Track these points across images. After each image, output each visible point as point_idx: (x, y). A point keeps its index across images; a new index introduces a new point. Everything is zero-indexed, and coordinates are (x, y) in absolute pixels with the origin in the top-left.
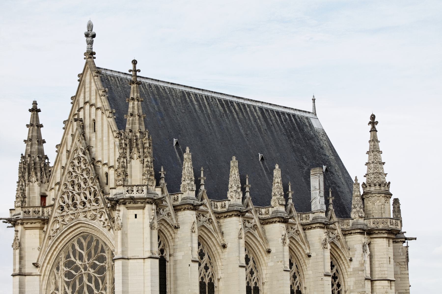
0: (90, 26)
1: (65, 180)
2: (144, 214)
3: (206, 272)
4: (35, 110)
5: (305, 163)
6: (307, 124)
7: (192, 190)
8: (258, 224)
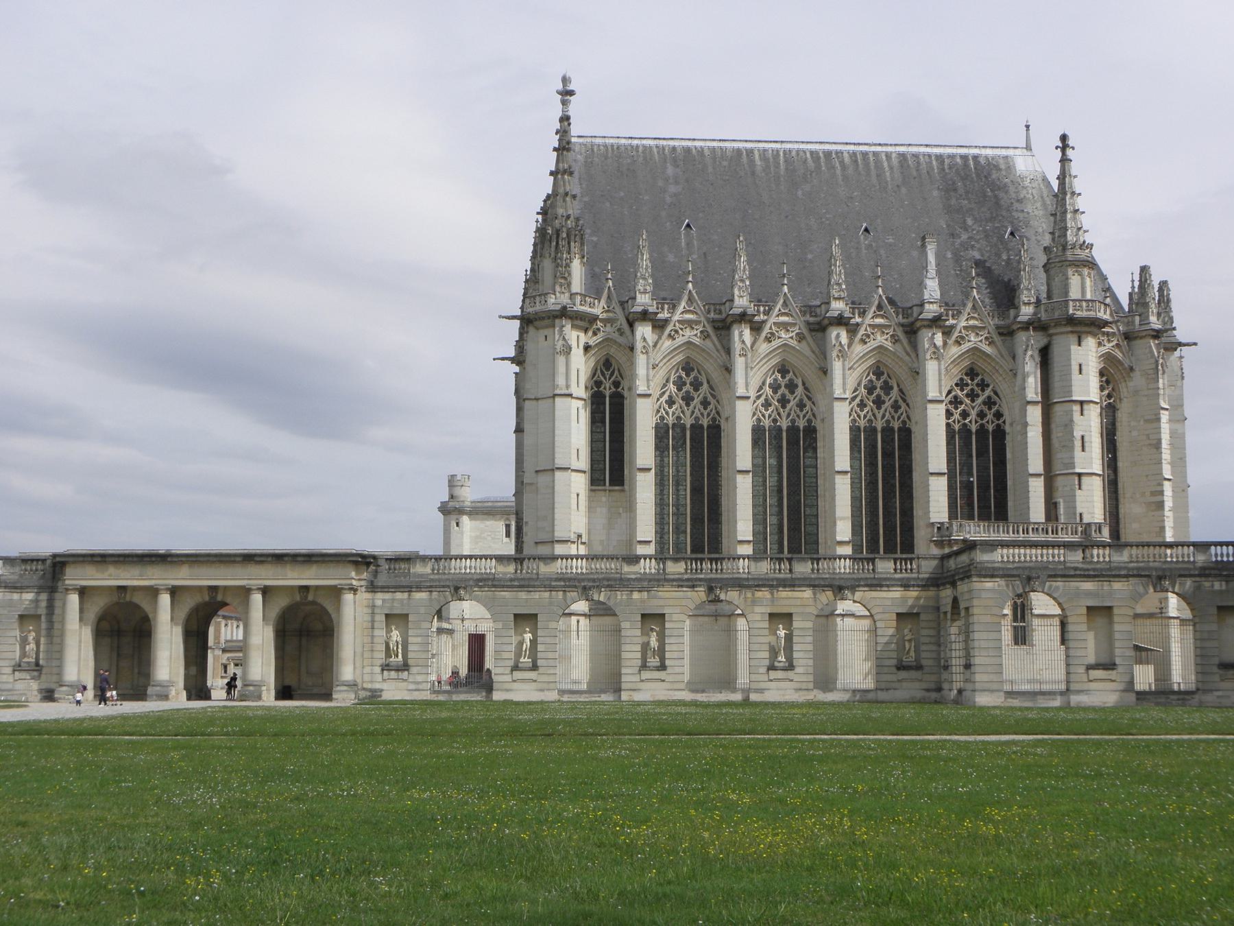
0: (565, 80)
3: (705, 409)
5: (966, 228)
6: (1003, 167)
7: (645, 292)
8: (805, 331)
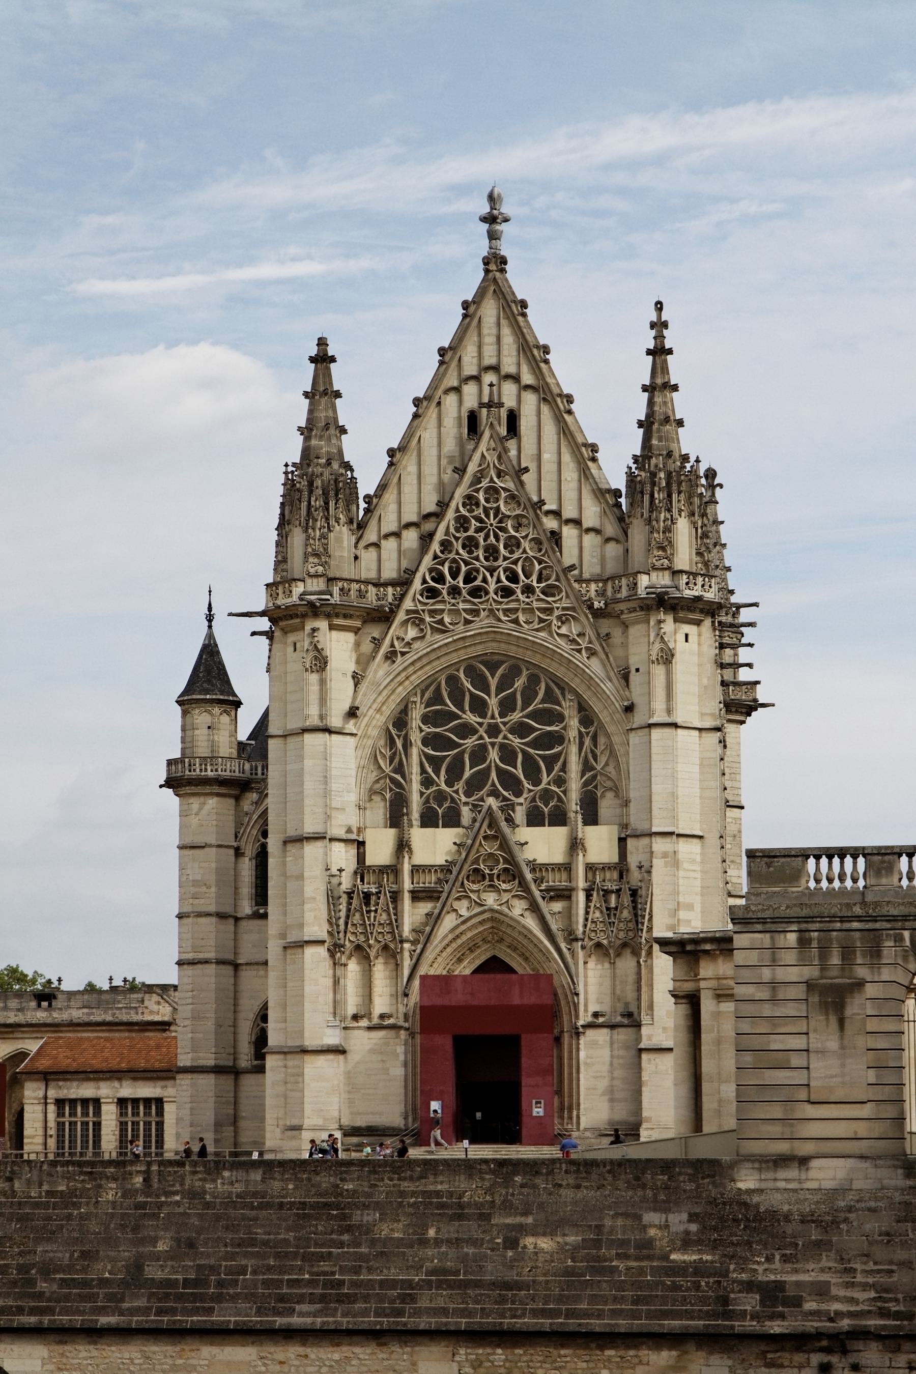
1: (447, 533)
2: (699, 635)
4: (322, 359)
